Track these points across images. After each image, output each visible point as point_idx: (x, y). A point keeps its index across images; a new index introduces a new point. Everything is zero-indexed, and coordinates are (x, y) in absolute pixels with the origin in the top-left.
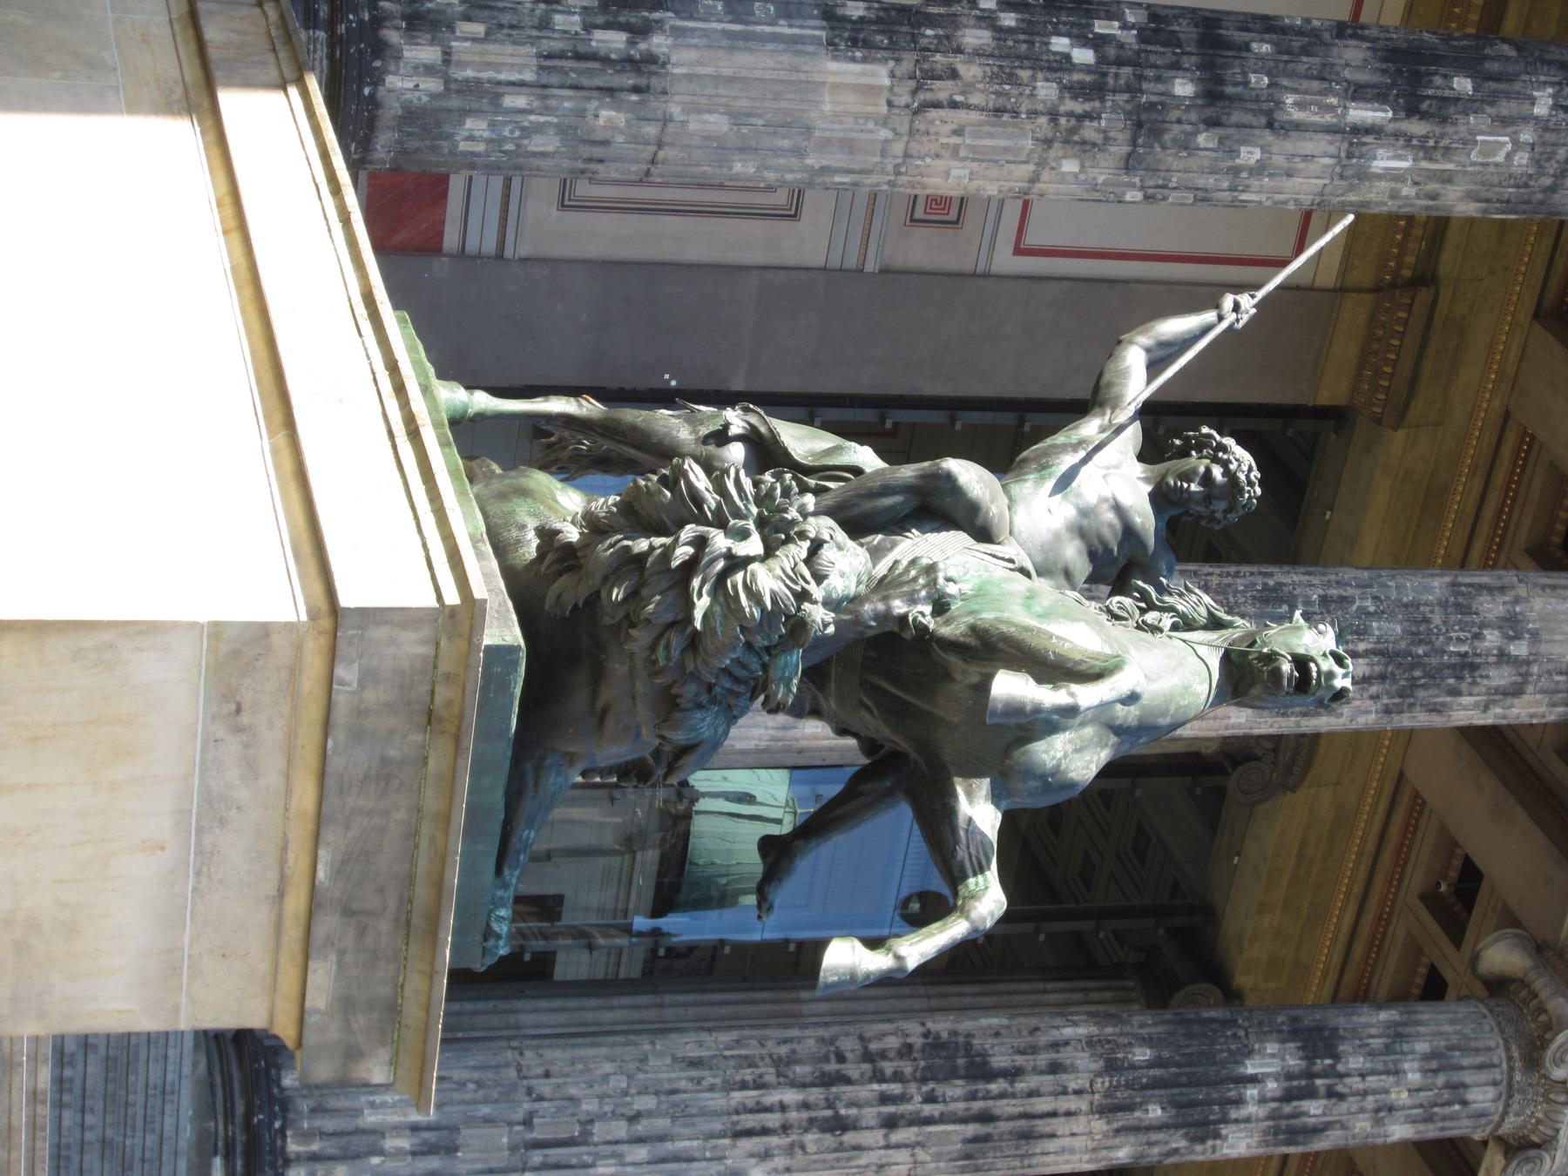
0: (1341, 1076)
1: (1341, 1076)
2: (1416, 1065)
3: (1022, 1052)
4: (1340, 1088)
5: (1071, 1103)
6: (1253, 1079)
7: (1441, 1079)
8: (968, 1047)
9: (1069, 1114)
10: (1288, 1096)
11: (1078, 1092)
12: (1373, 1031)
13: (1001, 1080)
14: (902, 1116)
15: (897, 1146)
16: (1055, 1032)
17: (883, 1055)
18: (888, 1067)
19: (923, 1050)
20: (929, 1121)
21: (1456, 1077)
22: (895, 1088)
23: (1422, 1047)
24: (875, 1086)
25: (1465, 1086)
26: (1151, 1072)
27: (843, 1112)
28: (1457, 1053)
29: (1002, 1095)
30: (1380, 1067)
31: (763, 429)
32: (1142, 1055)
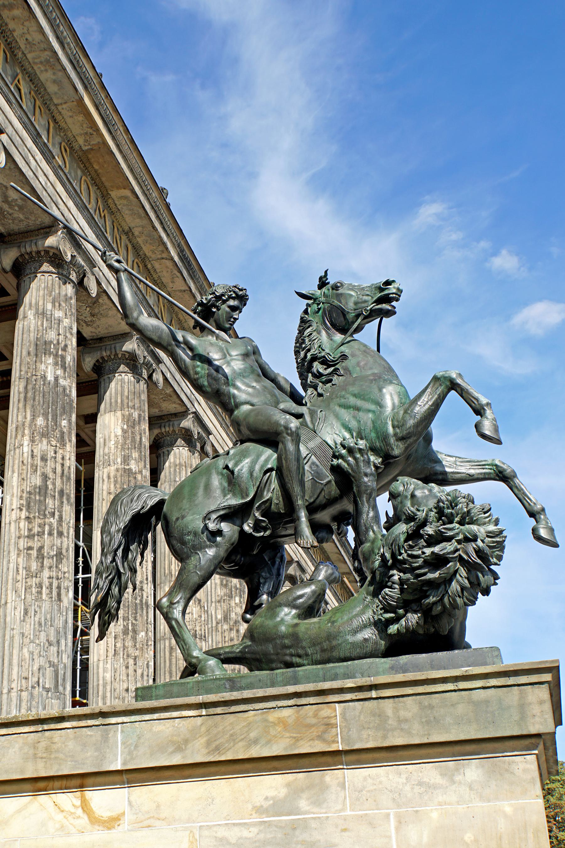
0: (58, 343)
1: (58, 343)
2: (56, 311)
3: (36, 470)
4: (63, 345)
5: (59, 456)
6: (56, 379)
7: (64, 305)
8: (30, 493)
9: (63, 458)
10: (64, 367)
11: (55, 453)
12: (39, 323)
13: (48, 483)
14: (58, 528)
15: (68, 533)
16: (25, 455)
17: (30, 530)
18: (36, 530)
19: (29, 512)
20: (61, 517)
21: (62, 298)
22: (47, 528)
23: (49, 306)
24: (46, 536)
25: (66, 295)
26: (50, 420)
27: (55, 553)
28: (53, 293)
29: (54, 484)
30: (56, 326)
31: (222, 513)
32: (40, 421)
